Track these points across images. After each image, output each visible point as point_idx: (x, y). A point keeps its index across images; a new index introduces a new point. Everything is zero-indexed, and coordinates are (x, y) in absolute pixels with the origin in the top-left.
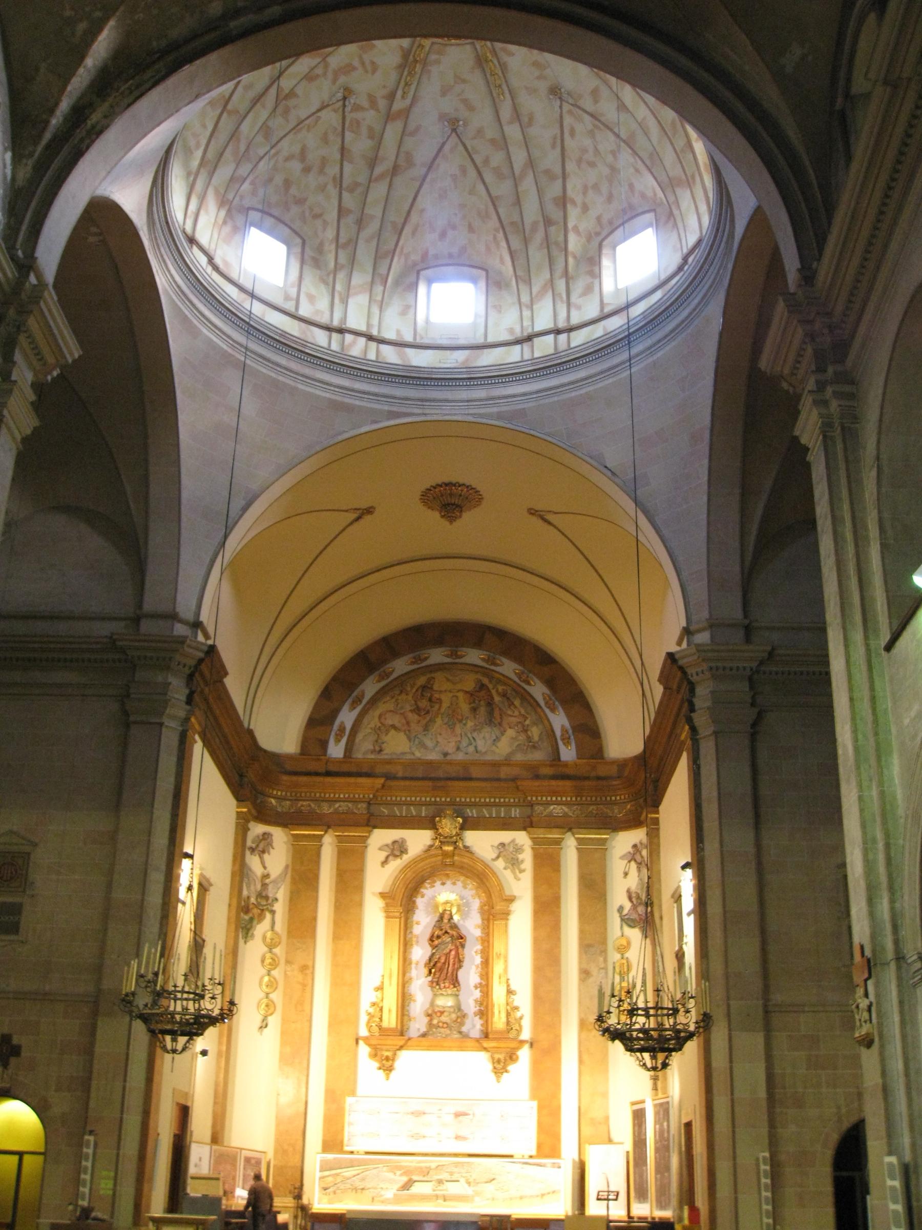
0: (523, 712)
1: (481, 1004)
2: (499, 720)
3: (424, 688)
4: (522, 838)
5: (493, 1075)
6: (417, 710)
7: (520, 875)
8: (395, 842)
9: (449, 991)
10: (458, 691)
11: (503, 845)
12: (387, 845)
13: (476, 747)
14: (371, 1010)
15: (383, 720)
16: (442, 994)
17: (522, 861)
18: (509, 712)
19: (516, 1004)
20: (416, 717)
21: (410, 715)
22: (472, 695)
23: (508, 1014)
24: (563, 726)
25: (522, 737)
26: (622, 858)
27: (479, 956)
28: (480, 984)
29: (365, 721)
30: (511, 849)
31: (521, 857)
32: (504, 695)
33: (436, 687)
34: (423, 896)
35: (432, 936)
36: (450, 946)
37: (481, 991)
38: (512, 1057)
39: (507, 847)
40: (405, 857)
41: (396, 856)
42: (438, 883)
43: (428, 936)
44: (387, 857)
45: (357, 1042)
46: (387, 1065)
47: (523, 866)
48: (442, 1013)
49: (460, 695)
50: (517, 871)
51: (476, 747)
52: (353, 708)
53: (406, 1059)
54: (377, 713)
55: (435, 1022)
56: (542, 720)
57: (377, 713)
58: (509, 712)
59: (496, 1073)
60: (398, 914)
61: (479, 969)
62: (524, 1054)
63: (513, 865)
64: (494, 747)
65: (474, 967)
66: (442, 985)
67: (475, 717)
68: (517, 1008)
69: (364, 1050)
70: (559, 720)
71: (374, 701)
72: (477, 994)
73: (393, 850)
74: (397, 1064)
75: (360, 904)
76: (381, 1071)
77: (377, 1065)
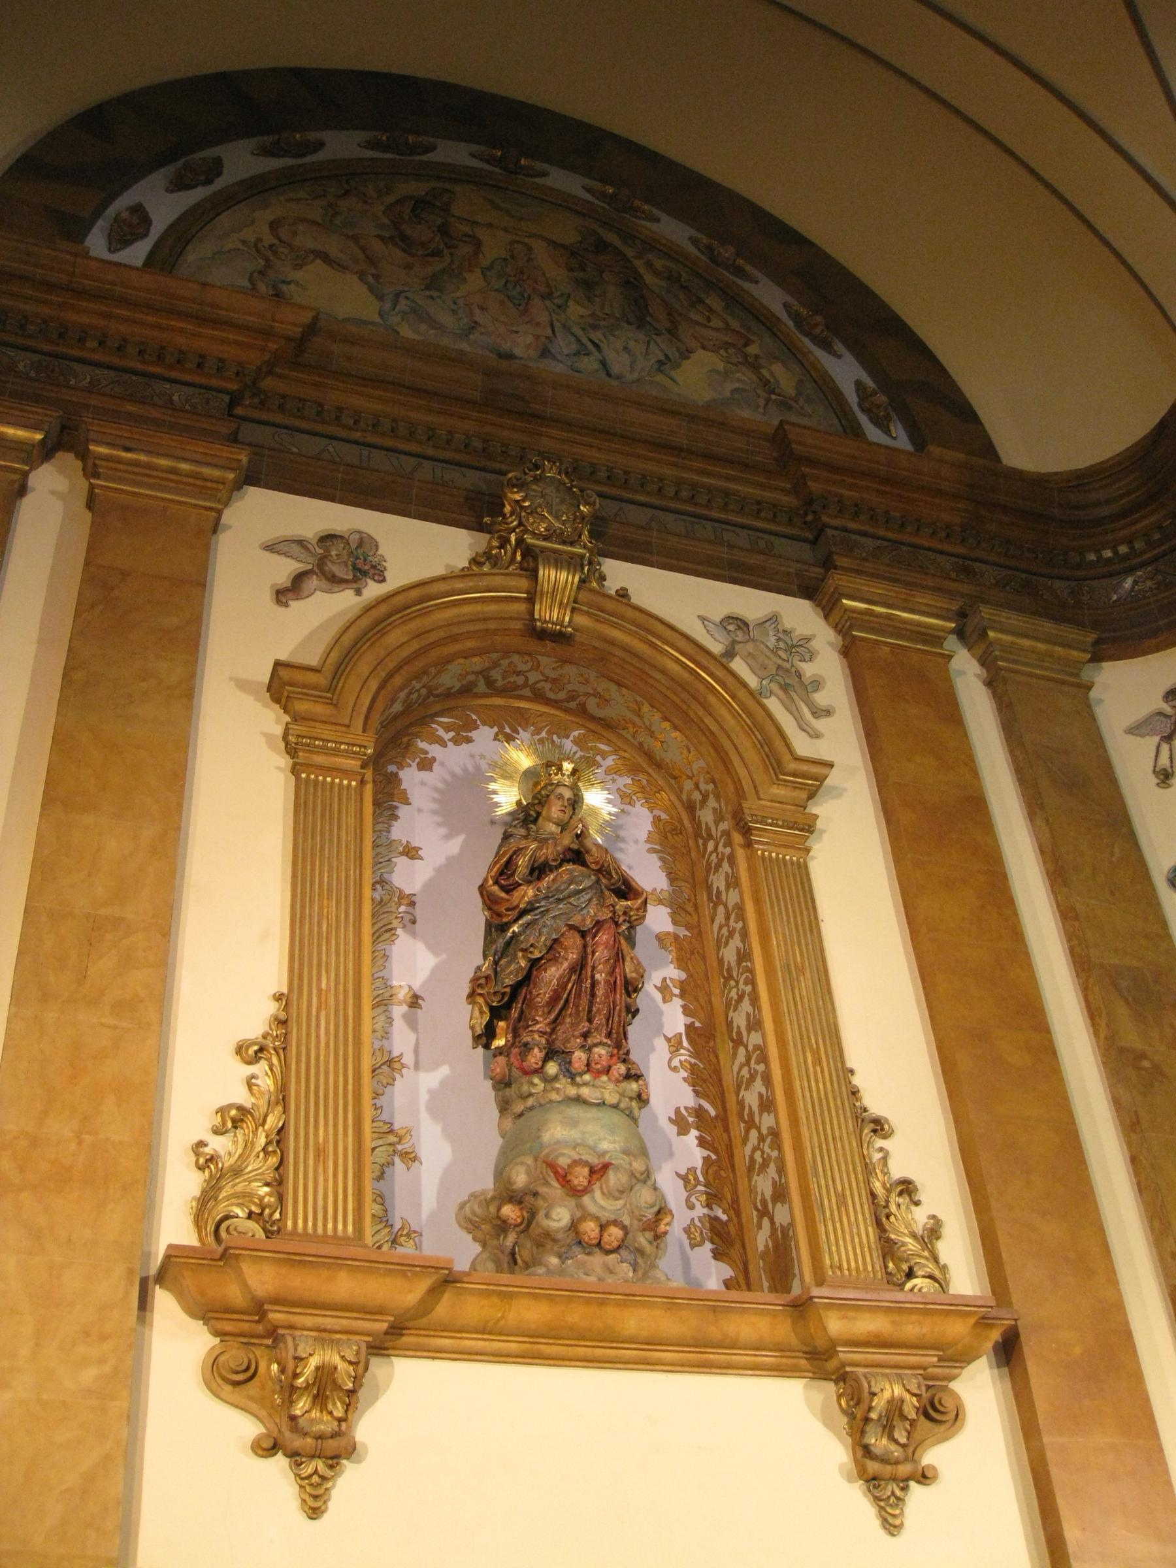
0: (735, 325)
1: (712, 1199)
2: (668, 325)
3: (420, 204)
4: (799, 615)
5: (857, 1502)
6: (404, 241)
7: (820, 724)
8: (328, 539)
9: (609, 1091)
10: (532, 236)
11: (741, 624)
12: (301, 543)
13: (603, 363)
14: (219, 1145)
15: (284, 233)
16: (579, 1100)
17: (818, 684)
18: (693, 315)
19: (897, 1170)
20: (398, 255)
21: (377, 247)
22: (573, 254)
23: (880, 1219)
24: (859, 385)
25: (745, 377)
26: (1136, 730)
27: (677, 1003)
28: (699, 1112)
29: (225, 220)
30: (772, 641)
31: (809, 670)
32: (672, 278)
33: (456, 210)
34: (426, 764)
35: (504, 873)
36: (590, 913)
37: (702, 1143)
38: (937, 1413)
39: (755, 633)
40: (373, 590)
41: (335, 581)
42: (484, 735)
43: (481, 868)
44: (298, 580)
45: (144, 1303)
46: (312, 1442)
47: (821, 698)
48: (598, 1171)
49: (539, 246)
50: (805, 711)
51: (603, 363)
52: (179, 185)
53: (418, 1405)
54: (269, 215)
55: (560, 1217)
56: (794, 354)
57: (269, 215)
58: (693, 315)
59: (872, 1482)
60: (353, 764)
61: (684, 1055)
62: (979, 1389)
63: (785, 688)
64: (660, 378)
65: (661, 1048)
66: (579, 1057)
67: (589, 299)
68: (907, 1188)
69: (178, 1344)
70: (846, 372)
71: (256, 189)
72: (690, 1151)
73: (322, 561)
74: (367, 1428)
75: (187, 693)
76: (280, 1461)
77: (249, 1428)
